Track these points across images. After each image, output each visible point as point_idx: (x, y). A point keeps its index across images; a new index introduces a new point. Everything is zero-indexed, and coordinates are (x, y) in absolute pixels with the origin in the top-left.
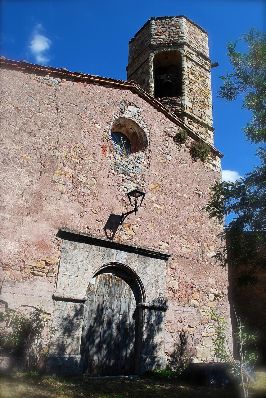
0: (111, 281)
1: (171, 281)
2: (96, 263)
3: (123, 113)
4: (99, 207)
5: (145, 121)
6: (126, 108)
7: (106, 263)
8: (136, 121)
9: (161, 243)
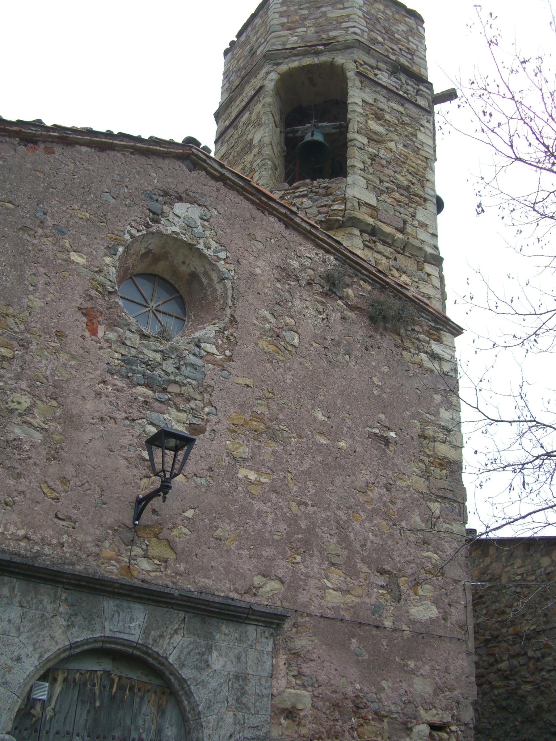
0: (97, 692)
1: (288, 690)
2: (47, 639)
3: (157, 221)
4: (64, 480)
5: (223, 241)
6: (166, 208)
7: (78, 640)
8: (194, 242)
9: (258, 580)
